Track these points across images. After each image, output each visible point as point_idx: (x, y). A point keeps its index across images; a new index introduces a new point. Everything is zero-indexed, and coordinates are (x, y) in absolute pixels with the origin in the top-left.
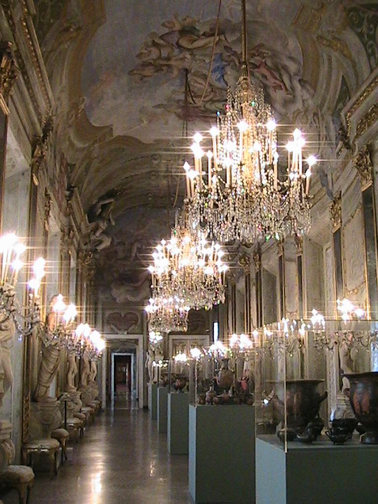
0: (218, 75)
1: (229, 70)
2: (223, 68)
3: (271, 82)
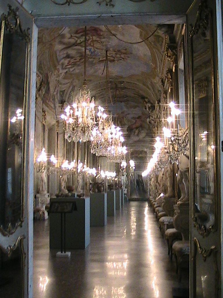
0: (93, 50)
2: (92, 53)
3: (72, 61)
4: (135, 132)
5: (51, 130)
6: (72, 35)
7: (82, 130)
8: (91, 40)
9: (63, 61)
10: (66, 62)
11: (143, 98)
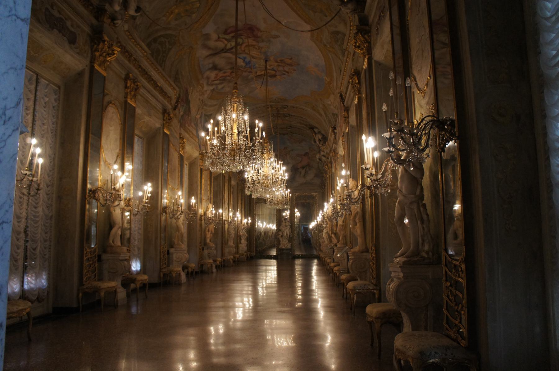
0: (248, 60)
1: (244, 65)
2: (246, 64)
4: (300, 173)
5: (192, 165)
6: (220, 36)
7: (230, 154)
8: (245, 45)
9: (208, 73)
10: (213, 75)
11: (312, 128)
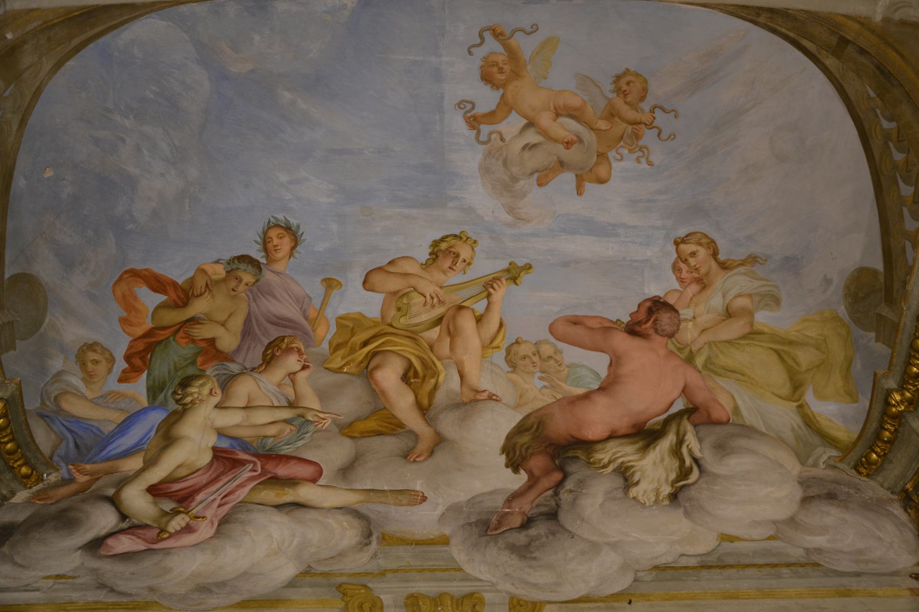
4: (626, 475)
